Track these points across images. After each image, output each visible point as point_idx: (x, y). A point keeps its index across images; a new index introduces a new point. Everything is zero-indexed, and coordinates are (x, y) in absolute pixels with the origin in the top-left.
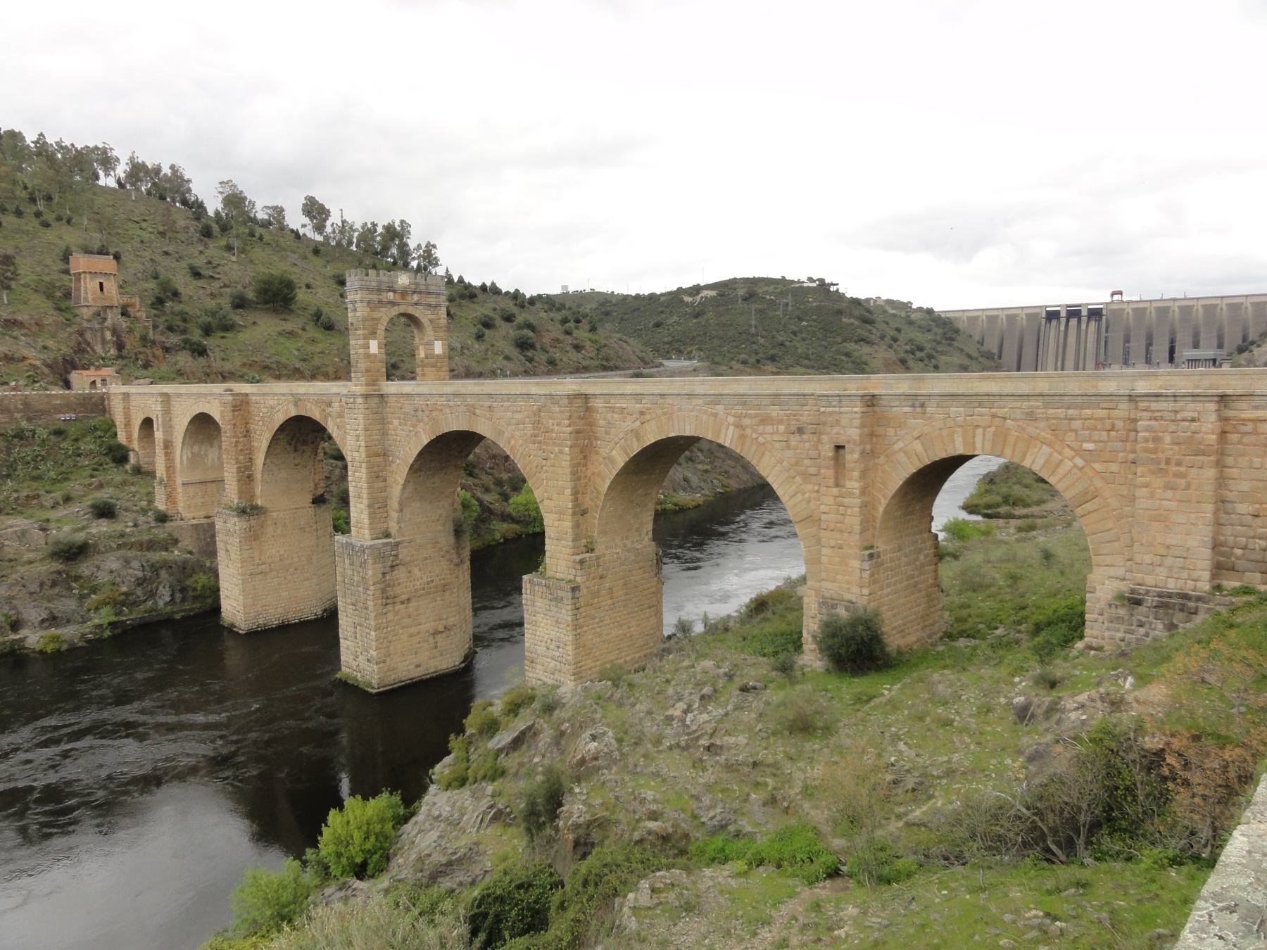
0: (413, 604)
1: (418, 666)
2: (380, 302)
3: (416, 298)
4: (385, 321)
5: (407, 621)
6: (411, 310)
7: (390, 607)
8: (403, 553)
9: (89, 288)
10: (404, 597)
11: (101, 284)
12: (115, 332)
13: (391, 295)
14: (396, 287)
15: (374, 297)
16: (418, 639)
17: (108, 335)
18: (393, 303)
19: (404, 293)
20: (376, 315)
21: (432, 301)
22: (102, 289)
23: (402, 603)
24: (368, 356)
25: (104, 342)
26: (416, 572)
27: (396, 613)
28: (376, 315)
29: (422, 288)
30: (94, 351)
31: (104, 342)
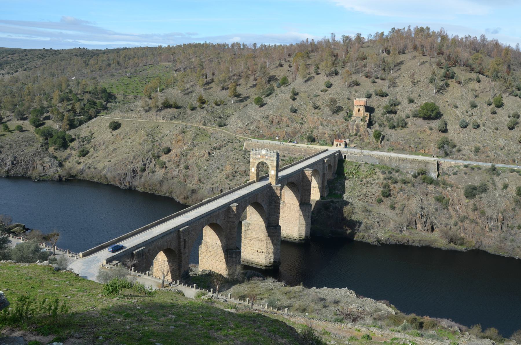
0: (252, 242)
1: (253, 258)
2: (256, 158)
3: (267, 157)
4: (257, 163)
5: (250, 245)
6: (265, 161)
7: (246, 240)
8: (250, 227)
9: (356, 109)
10: (250, 239)
11: (359, 110)
12: (357, 126)
13: (259, 156)
14: (261, 154)
15: (254, 156)
16: (253, 251)
17: (355, 126)
18: (259, 159)
19: (263, 156)
20: (255, 161)
21: (272, 159)
22: (359, 110)
23: (249, 240)
24: (252, 172)
25: (353, 129)
26: (254, 233)
27: (247, 242)
28: (255, 161)
29: (269, 155)
30: (349, 131)
31: (353, 129)
